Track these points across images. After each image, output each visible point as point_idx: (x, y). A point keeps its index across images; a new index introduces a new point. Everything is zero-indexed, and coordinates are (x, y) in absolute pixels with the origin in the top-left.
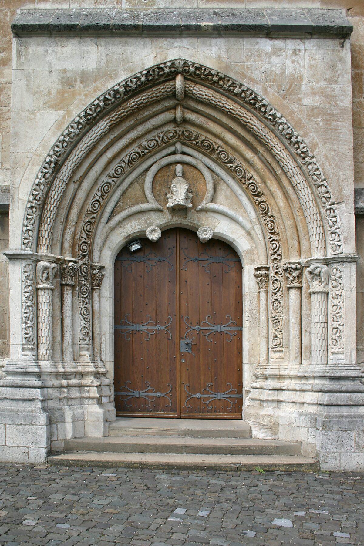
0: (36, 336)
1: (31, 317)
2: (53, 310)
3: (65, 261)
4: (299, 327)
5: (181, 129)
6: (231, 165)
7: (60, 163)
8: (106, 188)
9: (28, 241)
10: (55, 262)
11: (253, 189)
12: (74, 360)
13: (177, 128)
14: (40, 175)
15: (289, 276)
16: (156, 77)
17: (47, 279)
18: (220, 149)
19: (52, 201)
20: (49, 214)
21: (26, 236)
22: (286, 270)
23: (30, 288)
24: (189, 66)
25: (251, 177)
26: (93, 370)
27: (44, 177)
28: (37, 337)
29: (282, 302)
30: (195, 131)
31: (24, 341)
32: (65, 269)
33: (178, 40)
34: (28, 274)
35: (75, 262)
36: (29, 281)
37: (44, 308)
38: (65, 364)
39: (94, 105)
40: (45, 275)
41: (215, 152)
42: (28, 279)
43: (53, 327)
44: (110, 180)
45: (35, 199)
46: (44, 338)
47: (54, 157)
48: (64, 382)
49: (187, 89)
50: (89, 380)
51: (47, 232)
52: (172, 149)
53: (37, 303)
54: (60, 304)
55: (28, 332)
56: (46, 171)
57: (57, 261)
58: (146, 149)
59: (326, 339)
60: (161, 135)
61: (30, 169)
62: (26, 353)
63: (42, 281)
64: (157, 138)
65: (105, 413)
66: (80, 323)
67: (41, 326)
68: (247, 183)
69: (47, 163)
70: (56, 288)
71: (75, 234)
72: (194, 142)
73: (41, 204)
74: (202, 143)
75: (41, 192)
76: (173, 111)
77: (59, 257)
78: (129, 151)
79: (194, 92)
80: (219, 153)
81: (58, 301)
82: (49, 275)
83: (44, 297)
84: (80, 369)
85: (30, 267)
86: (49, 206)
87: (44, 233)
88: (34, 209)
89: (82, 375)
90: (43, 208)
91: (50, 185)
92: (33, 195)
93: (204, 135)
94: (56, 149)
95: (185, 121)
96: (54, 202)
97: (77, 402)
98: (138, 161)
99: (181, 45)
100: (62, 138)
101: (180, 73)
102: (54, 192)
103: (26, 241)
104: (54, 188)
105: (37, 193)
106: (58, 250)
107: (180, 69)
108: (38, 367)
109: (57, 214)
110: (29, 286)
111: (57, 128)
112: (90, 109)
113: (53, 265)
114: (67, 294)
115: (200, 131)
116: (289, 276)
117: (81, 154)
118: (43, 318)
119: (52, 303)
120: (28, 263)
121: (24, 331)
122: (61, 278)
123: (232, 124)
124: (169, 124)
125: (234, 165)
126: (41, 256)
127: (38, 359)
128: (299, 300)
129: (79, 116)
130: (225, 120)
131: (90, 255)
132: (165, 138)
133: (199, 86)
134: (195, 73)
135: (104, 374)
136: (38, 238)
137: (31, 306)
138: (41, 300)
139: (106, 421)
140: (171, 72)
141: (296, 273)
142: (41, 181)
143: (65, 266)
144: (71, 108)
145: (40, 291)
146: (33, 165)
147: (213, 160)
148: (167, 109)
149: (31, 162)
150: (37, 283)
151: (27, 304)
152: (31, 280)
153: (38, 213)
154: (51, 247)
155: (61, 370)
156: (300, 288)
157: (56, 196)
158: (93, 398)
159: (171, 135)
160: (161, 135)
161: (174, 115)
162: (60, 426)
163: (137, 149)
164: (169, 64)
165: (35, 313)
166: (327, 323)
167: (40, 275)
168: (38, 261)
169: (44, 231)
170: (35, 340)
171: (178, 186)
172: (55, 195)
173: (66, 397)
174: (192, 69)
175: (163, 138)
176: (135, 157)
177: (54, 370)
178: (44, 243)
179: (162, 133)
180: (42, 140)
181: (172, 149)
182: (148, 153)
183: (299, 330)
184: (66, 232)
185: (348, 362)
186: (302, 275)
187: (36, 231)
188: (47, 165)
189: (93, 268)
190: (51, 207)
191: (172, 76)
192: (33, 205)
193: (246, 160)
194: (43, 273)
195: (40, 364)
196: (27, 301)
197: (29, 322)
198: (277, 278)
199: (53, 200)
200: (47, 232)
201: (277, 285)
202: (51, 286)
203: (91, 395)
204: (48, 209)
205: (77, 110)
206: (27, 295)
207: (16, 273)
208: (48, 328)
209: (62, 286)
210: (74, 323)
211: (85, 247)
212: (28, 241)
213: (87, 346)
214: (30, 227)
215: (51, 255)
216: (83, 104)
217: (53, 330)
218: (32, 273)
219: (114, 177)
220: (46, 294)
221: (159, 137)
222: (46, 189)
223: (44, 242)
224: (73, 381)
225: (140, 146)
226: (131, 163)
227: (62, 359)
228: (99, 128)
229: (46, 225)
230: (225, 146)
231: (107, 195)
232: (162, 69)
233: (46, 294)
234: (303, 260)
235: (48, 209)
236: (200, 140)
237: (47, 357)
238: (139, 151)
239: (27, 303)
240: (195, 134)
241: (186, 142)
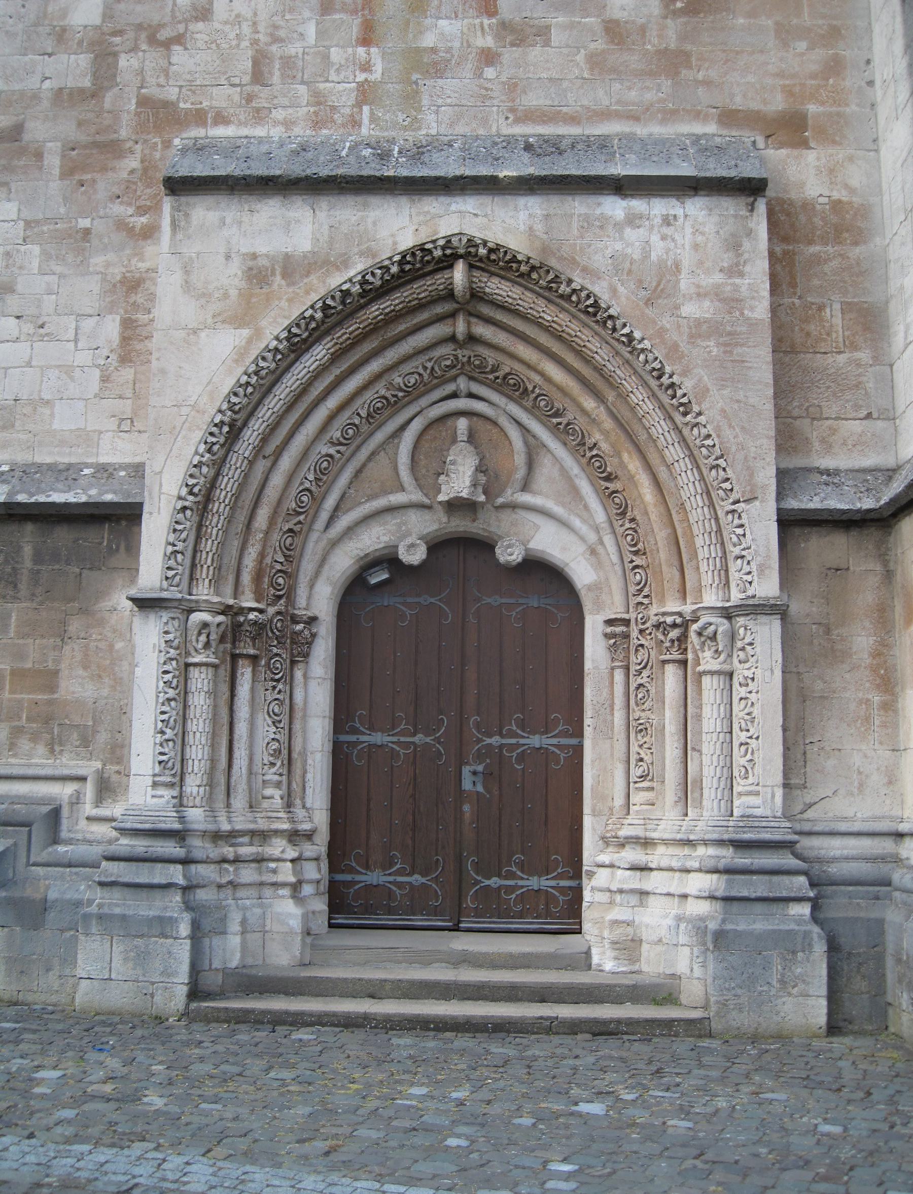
0: (179, 758)
1: (172, 720)
2: (215, 706)
3: (242, 609)
4: (683, 741)
5: (467, 353)
6: (559, 420)
7: (239, 424)
8: (325, 464)
9: (173, 572)
10: (222, 613)
11: (599, 468)
12: (251, 807)
13: (459, 351)
14: (202, 448)
15: (662, 638)
16: (418, 265)
17: (207, 645)
18: (537, 391)
19: (222, 496)
20: (215, 520)
21: (172, 563)
22: (657, 626)
23: (174, 663)
24: (477, 246)
25: (595, 444)
26: (286, 826)
27: (209, 451)
28: (183, 760)
29: (653, 691)
30: (491, 357)
31: (157, 769)
32: (241, 625)
33: (459, 199)
34: (170, 637)
35: (261, 611)
36: (172, 651)
37: (199, 702)
38: (232, 815)
39: (304, 318)
40: (203, 638)
41: (528, 395)
42: (171, 647)
43: (213, 739)
44: (332, 451)
45: (191, 493)
46: (196, 762)
47: (229, 413)
48: (229, 852)
49: (474, 286)
50: (278, 847)
51: (210, 554)
52: (450, 388)
54: (228, 694)
55: (166, 750)
56: (214, 440)
57: (226, 610)
58: (401, 390)
59: (728, 765)
60: (429, 365)
61: (184, 437)
62: (161, 791)
63: (196, 650)
64: (421, 371)
65: (305, 917)
66: (266, 730)
67: (190, 739)
68: (589, 454)
69: (216, 425)
70: (223, 661)
71: (262, 555)
72: (491, 377)
73: (200, 502)
74: (505, 378)
75: (203, 479)
76: (450, 321)
77: (231, 602)
78: (369, 395)
79: (487, 290)
80: (536, 398)
82: (211, 638)
83: (200, 680)
84: (262, 825)
85: (176, 623)
86: (217, 504)
87: (204, 556)
88: (188, 513)
89: (263, 836)
90: (205, 508)
91: (219, 465)
92: (187, 485)
93: (508, 365)
94: (234, 400)
95: (472, 339)
96: (225, 497)
97: (252, 892)
98: (387, 413)
99: (463, 209)
100: (245, 379)
101: (461, 257)
102: (226, 479)
103: (170, 573)
104: (226, 470)
105: (194, 481)
106: (229, 589)
107: (461, 251)
108: (182, 819)
109: (230, 520)
110: (172, 659)
111: (236, 361)
112: (298, 325)
113: (221, 618)
114: (243, 674)
115: (501, 358)
116: (662, 638)
117: (278, 406)
118: (195, 722)
119: (213, 693)
120: (172, 615)
121: (159, 749)
122: (234, 643)
123: (556, 347)
124: (444, 345)
125: (564, 421)
126: (197, 602)
127: (181, 805)
128: (682, 687)
129: (277, 338)
130: (544, 339)
131: (290, 595)
132: (436, 368)
133: (496, 280)
134: (488, 258)
135: (309, 836)
137: (174, 699)
138: (192, 686)
139: (309, 934)
140: (444, 255)
141: (674, 634)
142: (204, 460)
143: (242, 619)
144: (264, 323)
145: (191, 668)
146: (190, 429)
147: (526, 409)
148: (440, 319)
149: (187, 424)
150: (188, 654)
151: (167, 696)
152: (177, 648)
153: (196, 518)
154: (216, 582)
155: (226, 827)
156: (684, 663)
157: (230, 486)
158: (284, 885)
159: (448, 363)
160: (429, 365)
161: (451, 329)
162: (216, 941)
163: (383, 392)
164: (441, 242)
165: (181, 713)
166: (731, 733)
167: (194, 638)
168: (190, 611)
169: (204, 553)
170: (178, 766)
171: (459, 460)
172: (228, 484)
173: (230, 883)
174: (482, 251)
175: (433, 368)
176: (379, 405)
177: (211, 827)
178: (204, 576)
179: (430, 360)
180: (209, 383)
181: (450, 388)
182: (405, 397)
183: (681, 746)
185: (768, 813)
186: (686, 637)
187: (189, 554)
188: (214, 430)
189: (295, 620)
190: (220, 506)
191: (447, 262)
192: (187, 504)
193: (584, 412)
194: (200, 634)
195: (185, 814)
196: (166, 690)
197: (168, 731)
198: (643, 642)
199: (224, 493)
200: (210, 554)
201: (642, 655)
202: (212, 660)
203: (280, 878)
204: (215, 510)
205: (273, 327)
206: (168, 677)
207: (149, 638)
208: (203, 742)
209: (235, 657)
210: (256, 731)
211: (281, 581)
212: (173, 572)
213: (276, 778)
214: (180, 546)
215: (216, 599)
216: (285, 317)
217: (212, 746)
218: (178, 634)
219: (341, 444)
220: (203, 676)
221: (425, 368)
222: (212, 473)
223: (203, 574)
224: (246, 851)
225: (390, 386)
226: (373, 417)
227: (228, 805)
228: (313, 359)
229: (210, 542)
230: (546, 387)
231: (325, 478)
232: (430, 251)
233: (203, 676)
234: (688, 609)
235: (215, 510)
236: (501, 373)
237: (198, 800)
238: (388, 395)
239: (166, 693)
240: (491, 362)
241: (476, 375)
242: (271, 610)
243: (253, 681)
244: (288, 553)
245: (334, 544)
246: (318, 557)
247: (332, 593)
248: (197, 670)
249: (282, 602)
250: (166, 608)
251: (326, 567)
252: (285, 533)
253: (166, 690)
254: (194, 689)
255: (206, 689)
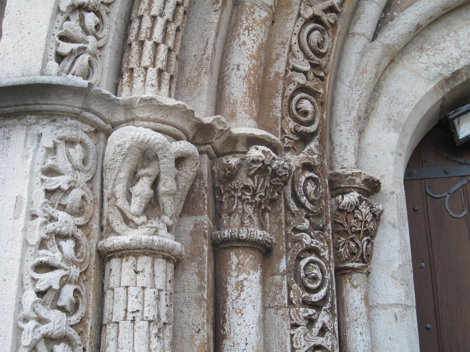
9: (75, 46)
17: (153, 206)
21: (72, 27)
32: (231, 175)
34: (61, 181)
36: (62, 216)
40: (143, 188)
42: (62, 207)
51: (160, 22)
53: (100, 326)
54: (207, 332)
81: (197, 318)
82: (162, 188)
85: (77, 153)
103: (66, 48)
110: (60, 236)
113: (184, 146)
114: (240, 286)
120: (67, 133)
136: (124, 47)
138: (115, 308)
143: (233, 161)
150: (106, 229)
151: (44, 329)
152: (78, 212)
154: (175, 76)
167: (120, 188)
178: (146, 61)
184: (235, 44)
194: (134, 178)
196: (43, 312)
200: (160, 22)
202: (166, 239)
206: (50, 279)
218: (82, 178)
220: (143, 280)
223: (143, 58)
233: (143, 280)
239: (41, 321)
242: (294, 160)
243: (265, 308)
244: (317, 60)
245: (395, 57)
246: (368, 77)
247: (400, 145)
248: (127, 265)
249: (313, 145)
250: (52, 116)
251: (383, 100)
252: (307, 22)
253: (43, 312)
254: (118, 314)
255: (150, 313)
